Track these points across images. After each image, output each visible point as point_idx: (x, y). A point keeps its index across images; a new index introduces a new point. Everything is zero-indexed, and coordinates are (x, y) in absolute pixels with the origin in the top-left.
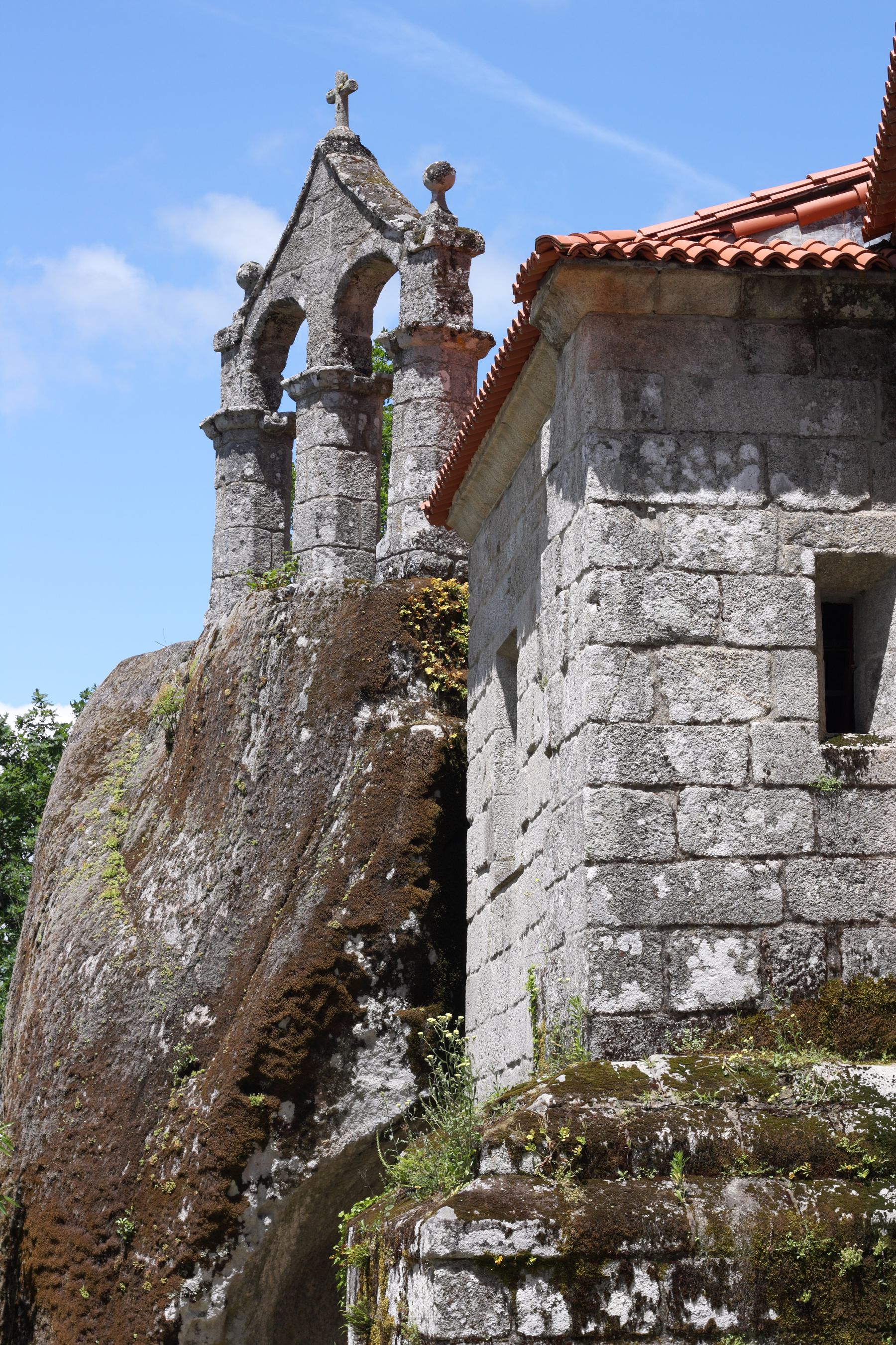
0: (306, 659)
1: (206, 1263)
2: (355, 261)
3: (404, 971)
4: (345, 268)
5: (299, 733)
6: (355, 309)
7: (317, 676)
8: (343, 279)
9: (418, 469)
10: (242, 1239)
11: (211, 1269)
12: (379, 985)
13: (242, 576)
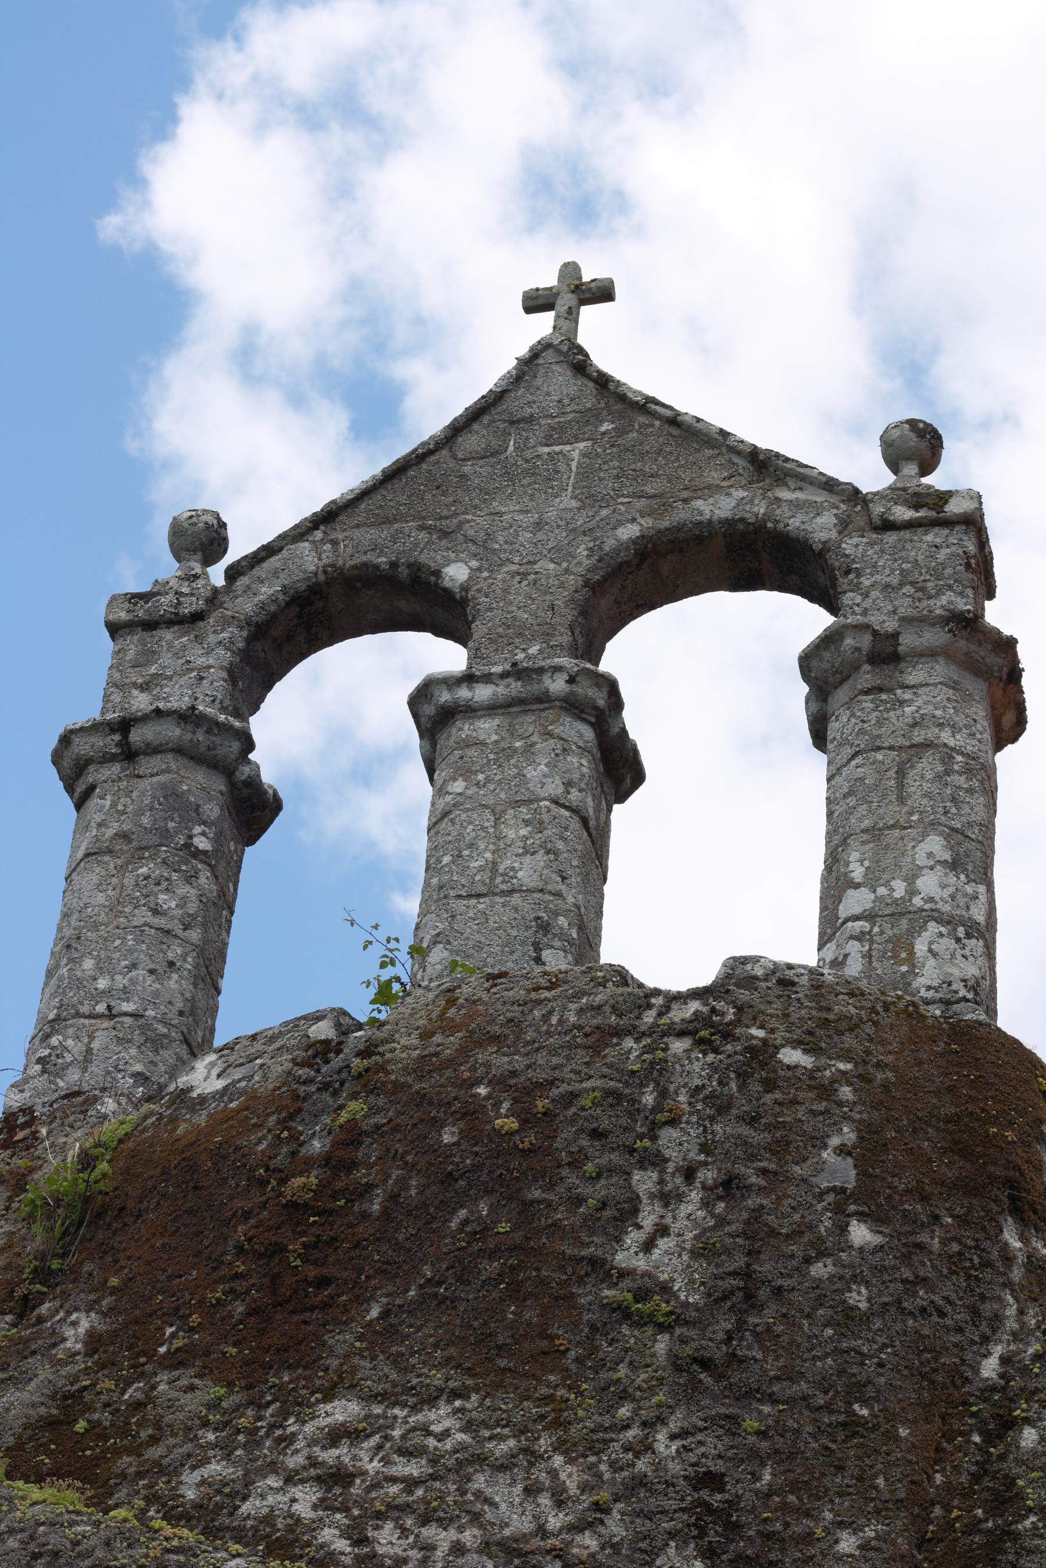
0: (826, 1091)
2: (664, 524)
4: (628, 532)
5: (844, 1229)
7: (867, 1132)
8: (617, 551)
13: (162, 1029)
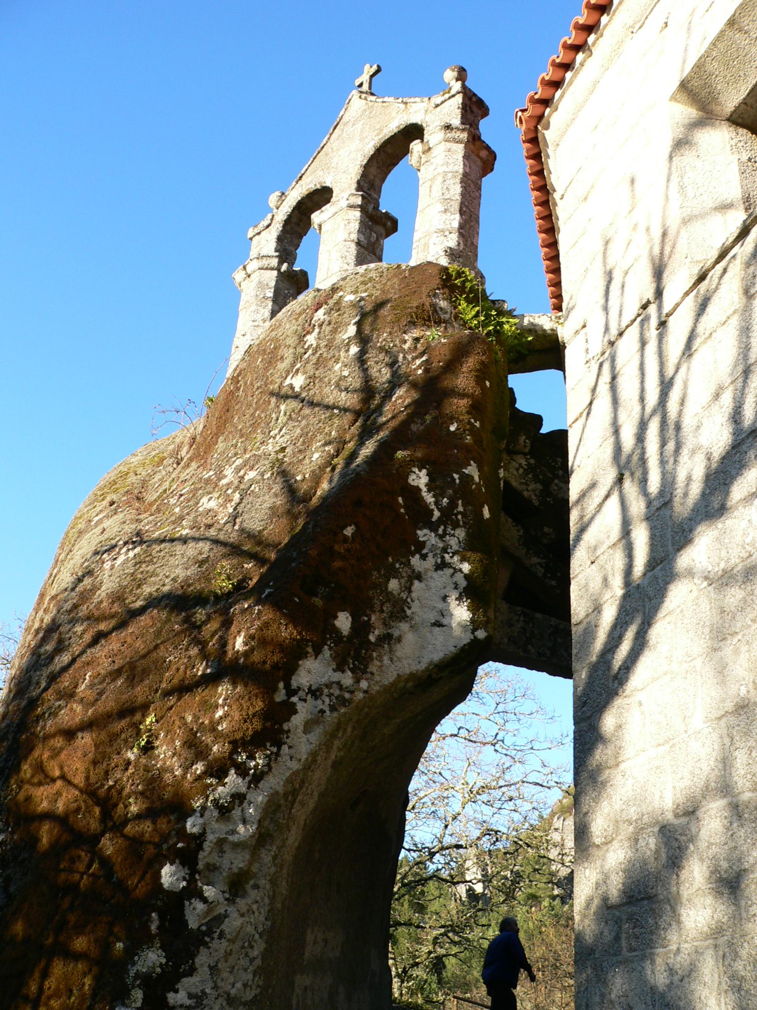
1: (242, 771)
3: (464, 514)
6: (372, 177)
9: (446, 211)
10: (285, 748)
11: (248, 779)
12: (440, 521)
